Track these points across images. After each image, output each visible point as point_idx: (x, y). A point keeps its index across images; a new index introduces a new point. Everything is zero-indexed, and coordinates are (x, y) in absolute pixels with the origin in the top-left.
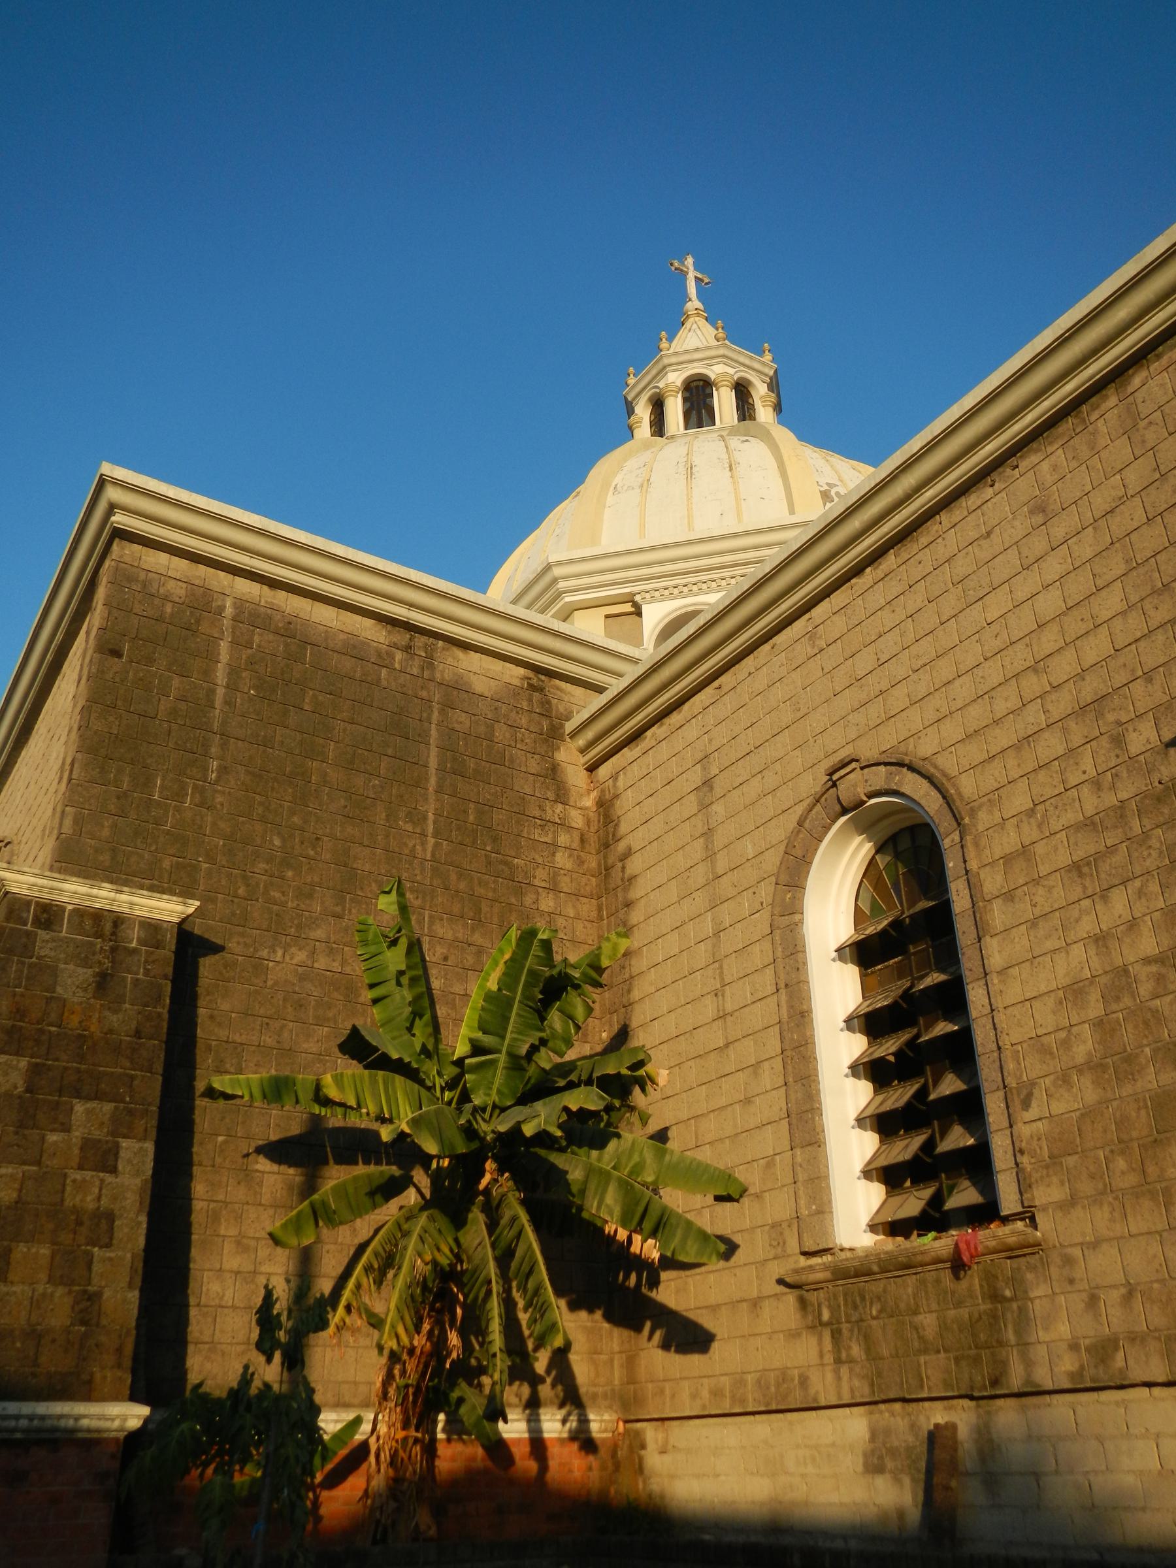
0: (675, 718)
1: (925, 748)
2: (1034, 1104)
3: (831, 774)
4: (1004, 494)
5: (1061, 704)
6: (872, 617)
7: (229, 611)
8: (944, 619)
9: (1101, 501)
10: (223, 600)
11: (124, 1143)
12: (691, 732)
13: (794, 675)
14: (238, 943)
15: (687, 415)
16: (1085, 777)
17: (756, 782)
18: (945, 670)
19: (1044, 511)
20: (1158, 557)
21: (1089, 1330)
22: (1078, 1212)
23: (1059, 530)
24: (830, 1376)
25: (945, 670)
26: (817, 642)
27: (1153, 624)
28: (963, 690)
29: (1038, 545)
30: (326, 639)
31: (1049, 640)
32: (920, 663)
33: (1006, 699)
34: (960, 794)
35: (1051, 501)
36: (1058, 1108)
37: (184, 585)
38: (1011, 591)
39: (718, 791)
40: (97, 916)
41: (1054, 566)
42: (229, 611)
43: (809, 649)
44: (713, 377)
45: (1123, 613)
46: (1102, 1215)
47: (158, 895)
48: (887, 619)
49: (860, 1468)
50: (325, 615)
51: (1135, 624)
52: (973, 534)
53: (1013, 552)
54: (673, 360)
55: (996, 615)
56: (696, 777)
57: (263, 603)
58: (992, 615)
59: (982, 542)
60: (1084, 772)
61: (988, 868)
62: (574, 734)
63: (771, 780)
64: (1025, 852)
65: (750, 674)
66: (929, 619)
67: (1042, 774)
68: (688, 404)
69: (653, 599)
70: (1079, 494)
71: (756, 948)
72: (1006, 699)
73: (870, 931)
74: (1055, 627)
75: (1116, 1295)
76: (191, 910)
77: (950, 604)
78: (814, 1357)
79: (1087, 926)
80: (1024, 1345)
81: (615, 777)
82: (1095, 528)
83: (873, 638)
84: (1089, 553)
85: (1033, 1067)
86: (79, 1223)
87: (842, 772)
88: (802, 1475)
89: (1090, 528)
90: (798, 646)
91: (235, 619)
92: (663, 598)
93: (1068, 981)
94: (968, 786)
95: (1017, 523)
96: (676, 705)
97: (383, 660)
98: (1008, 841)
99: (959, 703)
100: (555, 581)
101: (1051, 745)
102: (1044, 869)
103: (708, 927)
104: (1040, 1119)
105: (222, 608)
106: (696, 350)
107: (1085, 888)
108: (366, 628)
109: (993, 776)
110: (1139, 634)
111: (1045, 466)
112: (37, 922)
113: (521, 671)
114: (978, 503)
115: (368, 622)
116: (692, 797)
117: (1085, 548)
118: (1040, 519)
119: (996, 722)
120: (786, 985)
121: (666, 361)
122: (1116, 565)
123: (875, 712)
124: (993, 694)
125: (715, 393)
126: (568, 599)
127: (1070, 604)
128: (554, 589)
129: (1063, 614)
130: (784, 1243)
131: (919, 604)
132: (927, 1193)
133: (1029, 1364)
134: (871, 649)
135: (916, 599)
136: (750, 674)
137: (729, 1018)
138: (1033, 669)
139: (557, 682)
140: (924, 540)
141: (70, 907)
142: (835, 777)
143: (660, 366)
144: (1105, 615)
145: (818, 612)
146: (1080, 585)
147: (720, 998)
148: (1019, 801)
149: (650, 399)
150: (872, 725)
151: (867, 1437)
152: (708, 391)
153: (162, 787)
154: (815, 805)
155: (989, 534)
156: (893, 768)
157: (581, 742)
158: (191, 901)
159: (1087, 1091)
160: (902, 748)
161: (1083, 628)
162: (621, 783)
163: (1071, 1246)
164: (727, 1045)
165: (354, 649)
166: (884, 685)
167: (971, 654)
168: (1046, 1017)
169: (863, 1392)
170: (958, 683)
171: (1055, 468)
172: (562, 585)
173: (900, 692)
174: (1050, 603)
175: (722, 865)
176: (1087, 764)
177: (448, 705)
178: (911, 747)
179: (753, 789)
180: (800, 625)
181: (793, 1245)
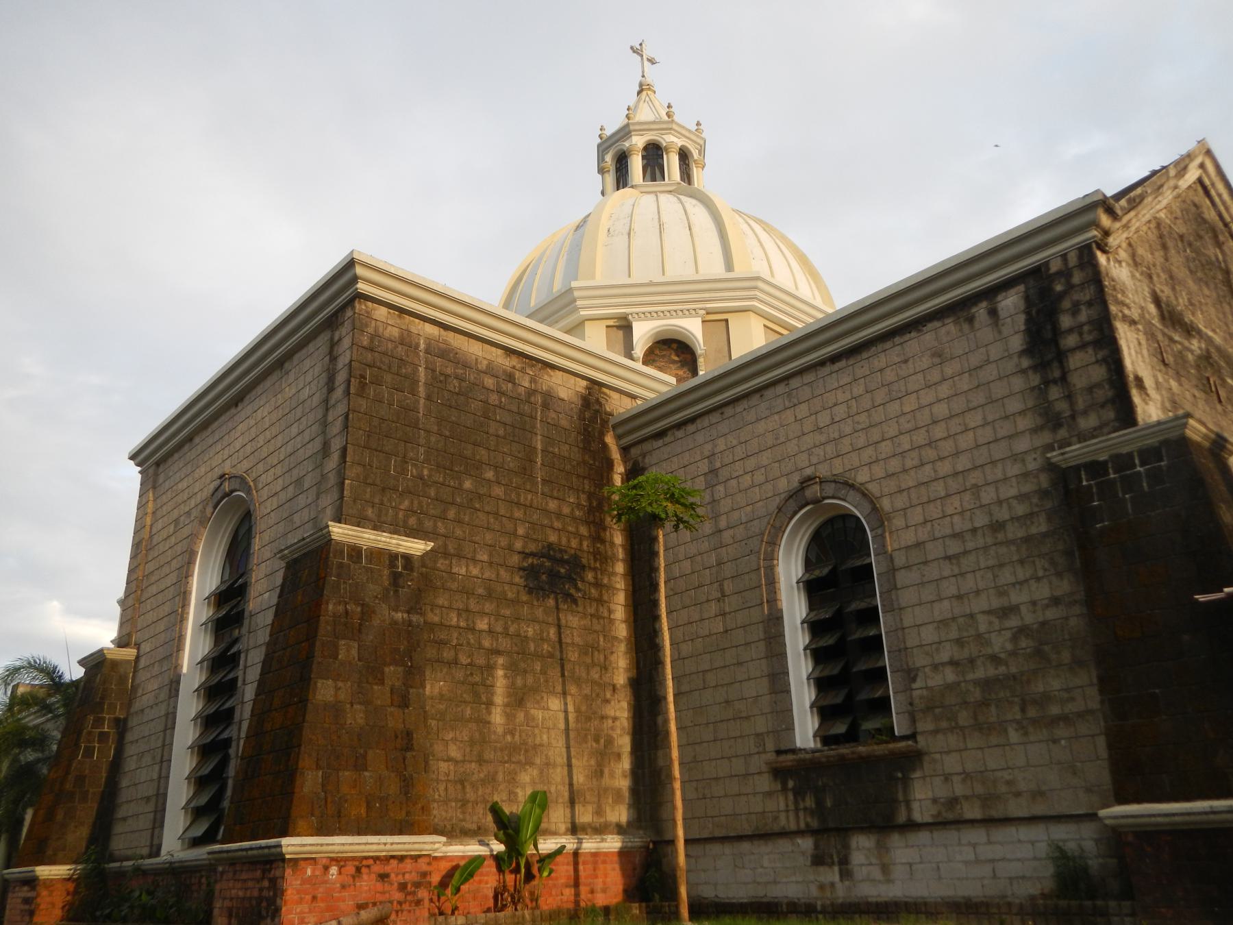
0: (691, 428)
1: (862, 477)
2: (919, 680)
3: (802, 483)
4: (916, 340)
5: (945, 468)
6: (830, 393)
7: (422, 346)
8: (876, 404)
9: (975, 359)
10: (419, 339)
11: (411, 691)
12: (700, 437)
13: (776, 417)
14: (442, 564)
15: (645, 168)
16: (957, 511)
17: (748, 477)
18: (875, 435)
19: (940, 356)
20: (1005, 399)
21: (942, 792)
22: (940, 737)
23: (949, 371)
24: (792, 815)
25: (875, 435)
26: (792, 400)
27: (999, 436)
28: (886, 448)
29: (935, 376)
30: (476, 363)
31: (939, 432)
32: (860, 427)
33: (912, 459)
34: (882, 510)
35: (946, 351)
36: (931, 683)
37: (397, 330)
38: (918, 398)
39: (722, 479)
40: (381, 552)
41: (944, 391)
42: (422, 346)
43: (787, 403)
44: (664, 145)
45: (983, 426)
46: (953, 740)
47: (412, 540)
48: (841, 397)
49: (809, 863)
50: (475, 349)
51: (986, 434)
52: (897, 359)
53: (920, 376)
54: (637, 127)
55: (909, 410)
56: (704, 467)
57: (441, 341)
58: (907, 409)
59: (903, 366)
60: (956, 508)
61: (897, 552)
62: (614, 427)
63: (759, 477)
64: (918, 545)
65: (745, 409)
66: (866, 403)
67: (932, 505)
68: (645, 162)
69: (640, 319)
70: (961, 352)
71: (746, 577)
72: (912, 459)
73: (817, 573)
74: (943, 424)
75: (959, 778)
76: (429, 548)
77: (880, 396)
78: (782, 806)
79: (953, 590)
80: (908, 803)
81: (644, 455)
82: (970, 375)
83: (830, 406)
84: (966, 388)
85: (920, 660)
86: (396, 737)
87: (809, 483)
88: (773, 868)
89: (967, 375)
90: (780, 400)
91: (427, 352)
92: (646, 319)
93: (939, 618)
94: (886, 504)
95: (924, 359)
96: (692, 420)
97: (510, 378)
98: (909, 537)
99: (884, 456)
100: (575, 300)
101: (939, 489)
102: (930, 557)
103: (713, 560)
104: (921, 688)
105: (417, 346)
106: (654, 122)
107: (952, 570)
108: (497, 356)
109: (900, 501)
110: (991, 440)
111: (943, 330)
112: (350, 557)
113: (584, 383)
114: (902, 340)
115: (500, 352)
116: (702, 478)
117: (964, 384)
118: (937, 360)
119: (905, 471)
120: (767, 601)
121: (632, 128)
122: (979, 398)
123: (830, 449)
124: (904, 454)
125: (665, 156)
126: (582, 313)
127: (953, 414)
128: (573, 305)
129: (948, 418)
130: (764, 745)
131: (861, 392)
132: (849, 720)
133: (909, 809)
134: (829, 411)
135: (858, 389)
136: (745, 409)
137: (728, 616)
138: (929, 444)
139: (605, 390)
140: (865, 355)
141: (365, 547)
142: (804, 485)
143: (627, 130)
144: (972, 425)
145: (795, 383)
146: (959, 405)
147: (722, 604)
148: (917, 516)
149: (616, 153)
150: (828, 457)
151: (813, 847)
152: (660, 153)
153: (395, 466)
154: (789, 499)
155: (906, 361)
156: (841, 486)
157: (620, 431)
158: (428, 543)
159: (950, 675)
160: (847, 475)
161: (959, 429)
162: (647, 460)
163: (936, 753)
164: (726, 631)
165: (490, 370)
166: (836, 435)
167: (892, 430)
168: (929, 634)
169: (815, 824)
170: (884, 443)
171: (948, 333)
172: (579, 303)
173: (847, 441)
174: (941, 410)
175: (723, 523)
176: (957, 504)
177: (546, 406)
178: (853, 475)
179: (747, 481)
180: (781, 389)
181: (770, 746)
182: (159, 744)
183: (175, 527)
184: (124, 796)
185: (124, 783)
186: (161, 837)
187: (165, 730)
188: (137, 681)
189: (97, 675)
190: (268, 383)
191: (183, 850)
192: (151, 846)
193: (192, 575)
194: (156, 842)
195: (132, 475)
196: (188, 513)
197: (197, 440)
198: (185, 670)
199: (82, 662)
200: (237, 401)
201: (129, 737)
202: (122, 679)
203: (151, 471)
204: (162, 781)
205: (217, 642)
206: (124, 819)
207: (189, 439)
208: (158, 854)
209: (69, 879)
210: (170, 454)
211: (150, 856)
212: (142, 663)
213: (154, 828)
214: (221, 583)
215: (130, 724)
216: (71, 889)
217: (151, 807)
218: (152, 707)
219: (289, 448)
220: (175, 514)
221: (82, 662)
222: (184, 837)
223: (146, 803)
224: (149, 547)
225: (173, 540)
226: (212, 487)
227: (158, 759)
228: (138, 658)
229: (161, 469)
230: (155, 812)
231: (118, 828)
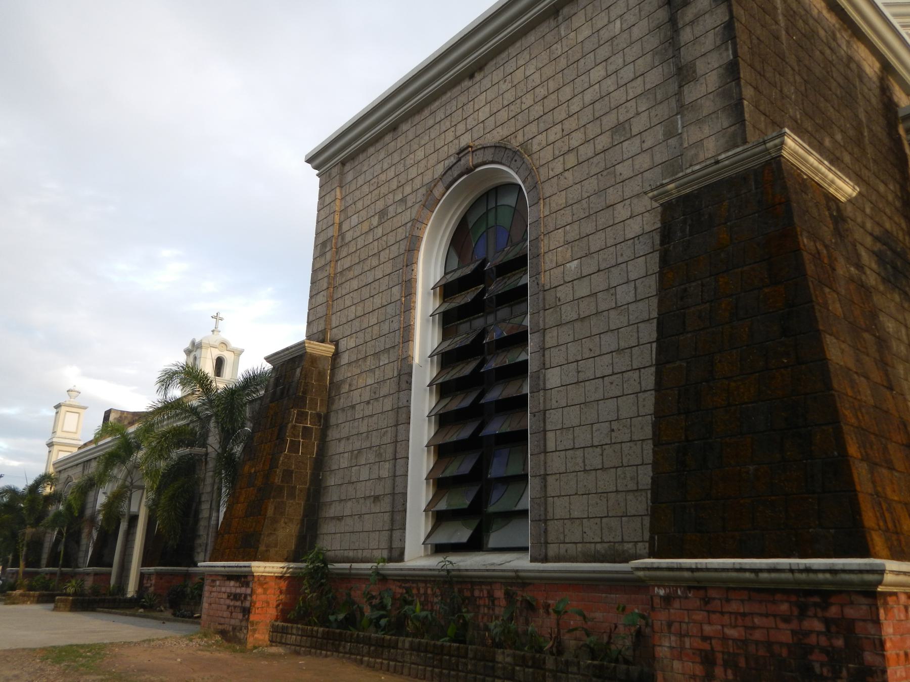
182: (388, 439)
183: (380, 218)
184: (332, 495)
185: (332, 480)
186: (403, 540)
187: (396, 425)
188: (339, 377)
189: (295, 369)
190: (531, 38)
191: (427, 556)
192: (391, 549)
193: (416, 263)
194: (396, 544)
195: (311, 179)
196: (403, 200)
197: (404, 127)
198: (416, 360)
199: (268, 359)
200: (470, 73)
201: (333, 434)
202: (321, 375)
203: (335, 171)
204: (398, 480)
205: (446, 335)
206: (340, 519)
207: (393, 128)
208: (400, 558)
209: (281, 578)
210: (363, 149)
211: (390, 560)
212: (344, 359)
213: (392, 530)
214: (446, 274)
215: (333, 421)
216: (284, 588)
217: (385, 505)
218: (368, 403)
219: (589, 97)
220: (380, 205)
221: (268, 359)
222: (428, 542)
223: (374, 502)
224: (339, 245)
225: (379, 232)
226: (440, 169)
227: (389, 455)
228: (336, 355)
229: (348, 167)
230: (393, 512)
231: (327, 528)
